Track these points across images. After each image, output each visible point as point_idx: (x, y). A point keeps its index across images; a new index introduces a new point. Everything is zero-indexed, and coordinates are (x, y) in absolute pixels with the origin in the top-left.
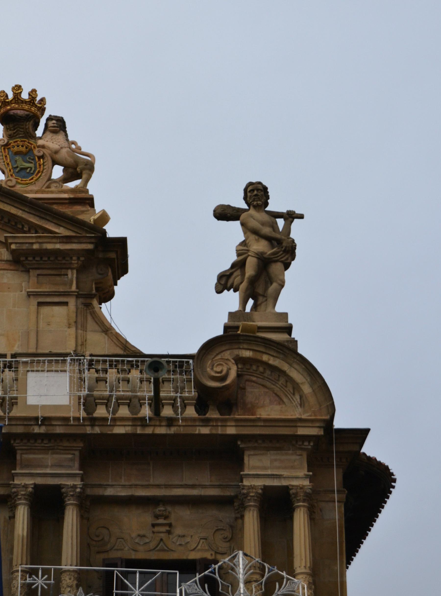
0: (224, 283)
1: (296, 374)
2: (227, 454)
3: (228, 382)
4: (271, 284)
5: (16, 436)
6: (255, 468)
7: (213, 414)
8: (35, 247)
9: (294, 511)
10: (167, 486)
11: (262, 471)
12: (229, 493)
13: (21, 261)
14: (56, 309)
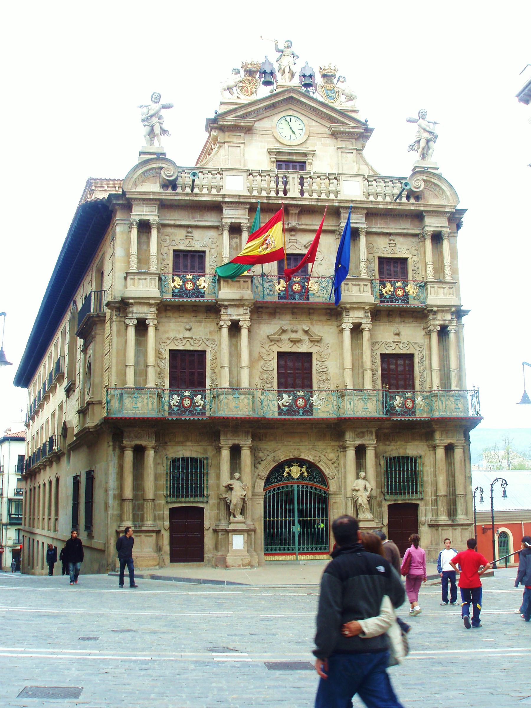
0: (412, 148)
1: (444, 187)
2: (418, 217)
3: (421, 189)
4: (430, 149)
5: (342, 207)
6: (430, 223)
7: (412, 201)
8: (342, 129)
9: (443, 240)
10: (395, 229)
11: (432, 224)
12: (418, 232)
13: (334, 135)
14: (349, 155)
